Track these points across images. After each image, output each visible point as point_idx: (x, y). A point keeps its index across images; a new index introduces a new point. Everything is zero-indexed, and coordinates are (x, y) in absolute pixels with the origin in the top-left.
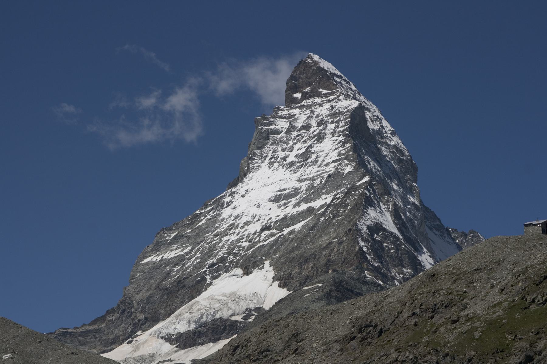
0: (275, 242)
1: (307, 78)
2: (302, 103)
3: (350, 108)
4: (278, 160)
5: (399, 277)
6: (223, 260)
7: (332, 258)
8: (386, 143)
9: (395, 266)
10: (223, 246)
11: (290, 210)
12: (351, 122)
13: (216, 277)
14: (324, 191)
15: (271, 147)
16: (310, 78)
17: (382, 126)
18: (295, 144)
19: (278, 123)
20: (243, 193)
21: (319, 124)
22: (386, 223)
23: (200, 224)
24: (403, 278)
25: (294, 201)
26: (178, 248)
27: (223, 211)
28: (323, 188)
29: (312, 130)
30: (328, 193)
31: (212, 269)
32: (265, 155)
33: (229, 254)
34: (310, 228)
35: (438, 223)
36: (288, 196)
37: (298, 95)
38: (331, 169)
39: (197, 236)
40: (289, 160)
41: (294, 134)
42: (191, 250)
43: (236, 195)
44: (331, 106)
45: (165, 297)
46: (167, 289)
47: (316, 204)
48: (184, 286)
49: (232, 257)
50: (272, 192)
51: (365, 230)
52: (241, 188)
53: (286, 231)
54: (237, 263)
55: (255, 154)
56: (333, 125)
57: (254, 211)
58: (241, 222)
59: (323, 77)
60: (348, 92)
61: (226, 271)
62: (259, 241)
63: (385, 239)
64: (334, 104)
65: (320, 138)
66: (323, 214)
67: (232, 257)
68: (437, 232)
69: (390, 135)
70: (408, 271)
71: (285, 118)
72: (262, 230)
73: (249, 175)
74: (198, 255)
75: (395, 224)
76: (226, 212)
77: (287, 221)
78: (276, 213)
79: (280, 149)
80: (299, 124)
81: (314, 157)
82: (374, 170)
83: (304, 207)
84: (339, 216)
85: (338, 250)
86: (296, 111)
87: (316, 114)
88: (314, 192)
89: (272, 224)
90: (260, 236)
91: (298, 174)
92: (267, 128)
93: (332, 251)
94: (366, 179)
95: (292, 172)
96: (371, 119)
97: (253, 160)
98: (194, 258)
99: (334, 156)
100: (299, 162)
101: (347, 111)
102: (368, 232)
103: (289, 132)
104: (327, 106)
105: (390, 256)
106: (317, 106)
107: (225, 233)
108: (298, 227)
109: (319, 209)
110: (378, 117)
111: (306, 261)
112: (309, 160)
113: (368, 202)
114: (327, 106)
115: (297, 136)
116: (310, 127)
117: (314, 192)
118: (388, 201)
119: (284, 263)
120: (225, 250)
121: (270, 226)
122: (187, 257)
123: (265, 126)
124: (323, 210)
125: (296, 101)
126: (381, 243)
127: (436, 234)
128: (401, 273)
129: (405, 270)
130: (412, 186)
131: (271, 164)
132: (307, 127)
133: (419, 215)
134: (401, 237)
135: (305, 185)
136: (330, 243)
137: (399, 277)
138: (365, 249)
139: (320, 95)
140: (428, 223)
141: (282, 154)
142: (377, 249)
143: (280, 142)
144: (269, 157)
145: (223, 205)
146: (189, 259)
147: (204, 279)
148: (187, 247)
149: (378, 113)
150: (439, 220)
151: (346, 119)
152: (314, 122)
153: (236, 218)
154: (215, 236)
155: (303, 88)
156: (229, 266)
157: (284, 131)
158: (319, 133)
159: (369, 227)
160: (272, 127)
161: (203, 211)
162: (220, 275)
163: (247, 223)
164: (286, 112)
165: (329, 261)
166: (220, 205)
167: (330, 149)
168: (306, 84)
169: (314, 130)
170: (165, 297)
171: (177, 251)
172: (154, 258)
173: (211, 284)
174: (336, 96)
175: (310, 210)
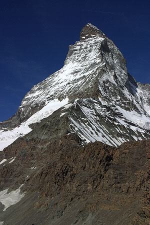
6: (51, 96)
9: (113, 96)
11: (78, 77)
21: (90, 47)
36: (76, 72)
38: (93, 62)
40: (79, 59)
47: (86, 74)
50: (72, 70)
52: (61, 70)
53: (75, 84)
55: (68, 58)
57: (66, 78)
65: (90, 51)
76: (56, 79)
77: (75, 81)
78: (72, 78)
83: (82, 75)
86: (83, 43)
94: (104, 64)
99: (95, 57)
103: (80, 50)
104: (94, 40)
114: (94, 40)
118: (112, 72)
132: (86, 48)
134: (117, 85)
138: (101, 90)
139: (91, 37)
141: (77, 58)
147: (44, 103)
149: (112, 43)
152: (89, 46)
159: (104, 82)
166: (53, 76)
167: (94, 56)
172: (30, 96)
175: (84, 77)
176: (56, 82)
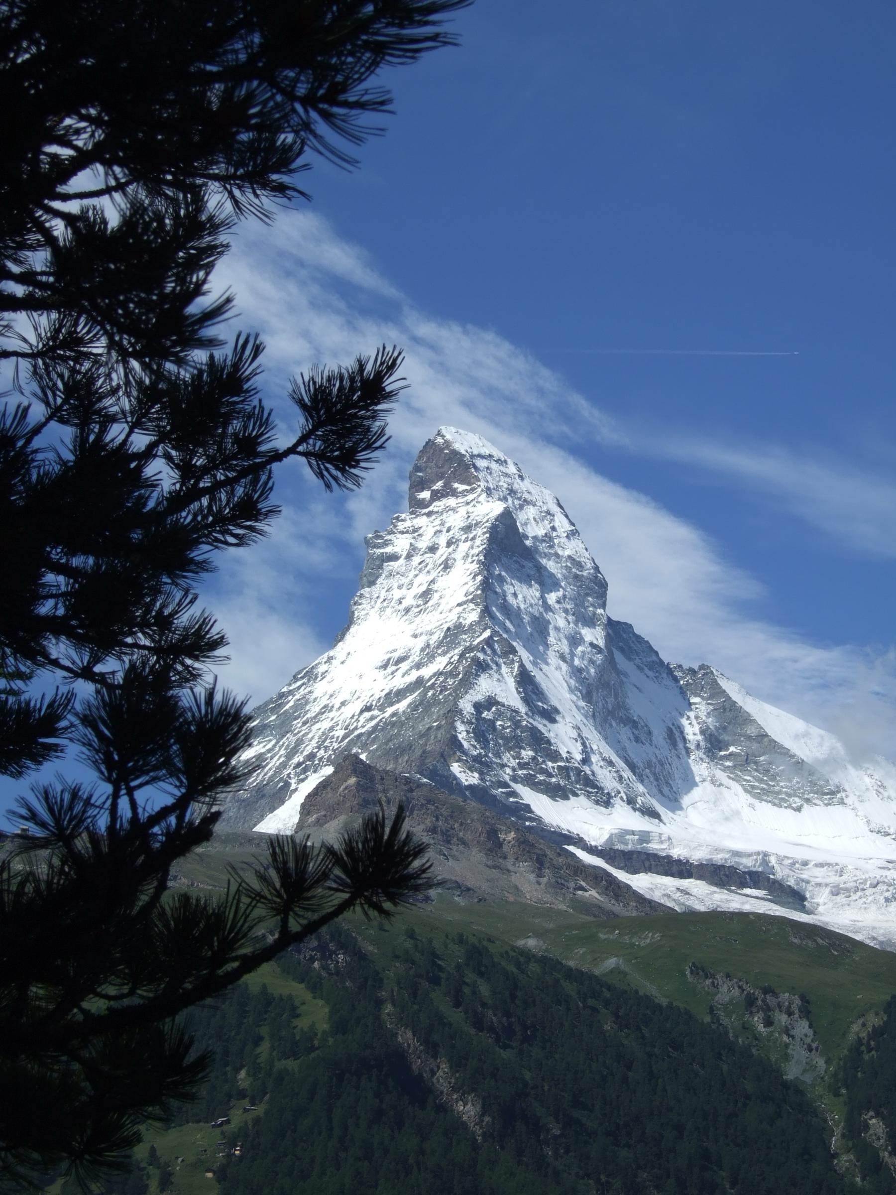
0: (375, 728)
1: (437, 466)
2: (431, 508)
3: (491, 515)
4: (392, 604)
5: (514, 763)
6: (311, 756)
7: (428, 748)
8: (557, 555)
9: (509, 749)
10: (312, 738)
11: (399, 682)
12: (490, 540)
13: (303, 780)
14: (439, 651)
15: (385, 582)
16: (442, 467)
17: (553, 529)
18: (416, 576)
19: (396, 542)
20: (343, 658)
21: (449, 544)
22: (503, 694)
23: (287, 707)
24: (519, 764)
25: (404, 666)
26: (259, 743)
27: (316, 685)
28: (438, 647)
29: (439, 552)
30: (444, 654)
31: (298, 770)
32: (376, 596)
33: (319, 748)
34: (414, 707)
35: (654, 658)
37: (425, 495)
38: (451, 619)
39: (283, 724)
40: (406, 603)
41: (416, 560)
42: (274, 746)
43: (333, 661)
44: (468, 513)
45: (242, 811)
46: (244, 801)
47: (427, 672)
48: (264, 796)
49: (322, 752)
51: (468, 709)
53: (390, 711)
54: (329, 759)
55: (362, 596)
56: (469, 543)
58: (337, 702)
59: (459, 464)
60: (499, 481)
61: (315, 772)
62: (356, 728)
63: (500, 716)
64: (471, 510)
65: (447, 566)
66: (432, 686)
67: (322, 752)
68: (650, 673)
69: (564, 540)
70: (527, 754)
71: (407, 532)
72: (362, 712)
73: (353, 629)
74: (282, 752)
75: (519, 693)
79: (395, 585)
80: (423, 544)
81: (436, 596)
82: (522, 606)
83: (414, 676)
84: (446, 689)
85: (435, 737)
86: (422, 521)
87: (447, 525)
88: (429, 654)
89: (374, 703)
90: (358, 720)
91: (413, 626)
92: (382, 551)
93: (428, 740)
94: (487, 634)
95: (408, 622)
96: (535, 519)
97: (360, 604)
98: (277, 757)
100: (418, 606)
101: (487, 521)
102: (473, 711)
104: (463, 511)
105: (503, 737)
106: (450, 512)
107: (316, 719)
108: (402, 706)
109: (430, 679)
110: (548, 512)
111: (403, 751)
112: (430, 604)
113: (482, 667)
114: (463, 511)
115: (420, 563)
116: (437, 548)
117: (429, 654)
118: (513, 662)
119: (380, 757)
120: (314, 743)
121: (371, 705)
122: (269, 755)
123: (379, 548)
124: (433, 680)
125: (423, 504)
126: (492, 723)
127: (648, 677)
128: (518, 756)
129: (523, 753)
130: (594, 614)
131: (383, 609)
132: (433, 549)
133: (599, 658)
135: (420, 643)
136: (430, 728)
137: (514, 763)
139: (454, 493)
140: (638, 661)
141: (397, 594)
142: (482, 731)
143: (398, 573)
144: (381, 600)
145: (316, 678)
146: (272, 758)
147: (287, 784)
148: (270, 741)
150: (656, 653)
151: (484, 533)
152: (442, 540)
153: (331, 696)
154: (304, 723)
155: (434, 482)
156: (319, 764)
157: (405, 554)
158: (447, 560)
160: (388, 550)
161: (291, 688)
162: (307, 777)
163: (343, 704)
164: (408, 524)
165: (424, 752)
168: (438, 476)
169: (443, 552)
170: (242, 811)
171: (258, 747)
173: (296, 790)
174: (475, 495)
175: (420, 682)
176: (324, 701)
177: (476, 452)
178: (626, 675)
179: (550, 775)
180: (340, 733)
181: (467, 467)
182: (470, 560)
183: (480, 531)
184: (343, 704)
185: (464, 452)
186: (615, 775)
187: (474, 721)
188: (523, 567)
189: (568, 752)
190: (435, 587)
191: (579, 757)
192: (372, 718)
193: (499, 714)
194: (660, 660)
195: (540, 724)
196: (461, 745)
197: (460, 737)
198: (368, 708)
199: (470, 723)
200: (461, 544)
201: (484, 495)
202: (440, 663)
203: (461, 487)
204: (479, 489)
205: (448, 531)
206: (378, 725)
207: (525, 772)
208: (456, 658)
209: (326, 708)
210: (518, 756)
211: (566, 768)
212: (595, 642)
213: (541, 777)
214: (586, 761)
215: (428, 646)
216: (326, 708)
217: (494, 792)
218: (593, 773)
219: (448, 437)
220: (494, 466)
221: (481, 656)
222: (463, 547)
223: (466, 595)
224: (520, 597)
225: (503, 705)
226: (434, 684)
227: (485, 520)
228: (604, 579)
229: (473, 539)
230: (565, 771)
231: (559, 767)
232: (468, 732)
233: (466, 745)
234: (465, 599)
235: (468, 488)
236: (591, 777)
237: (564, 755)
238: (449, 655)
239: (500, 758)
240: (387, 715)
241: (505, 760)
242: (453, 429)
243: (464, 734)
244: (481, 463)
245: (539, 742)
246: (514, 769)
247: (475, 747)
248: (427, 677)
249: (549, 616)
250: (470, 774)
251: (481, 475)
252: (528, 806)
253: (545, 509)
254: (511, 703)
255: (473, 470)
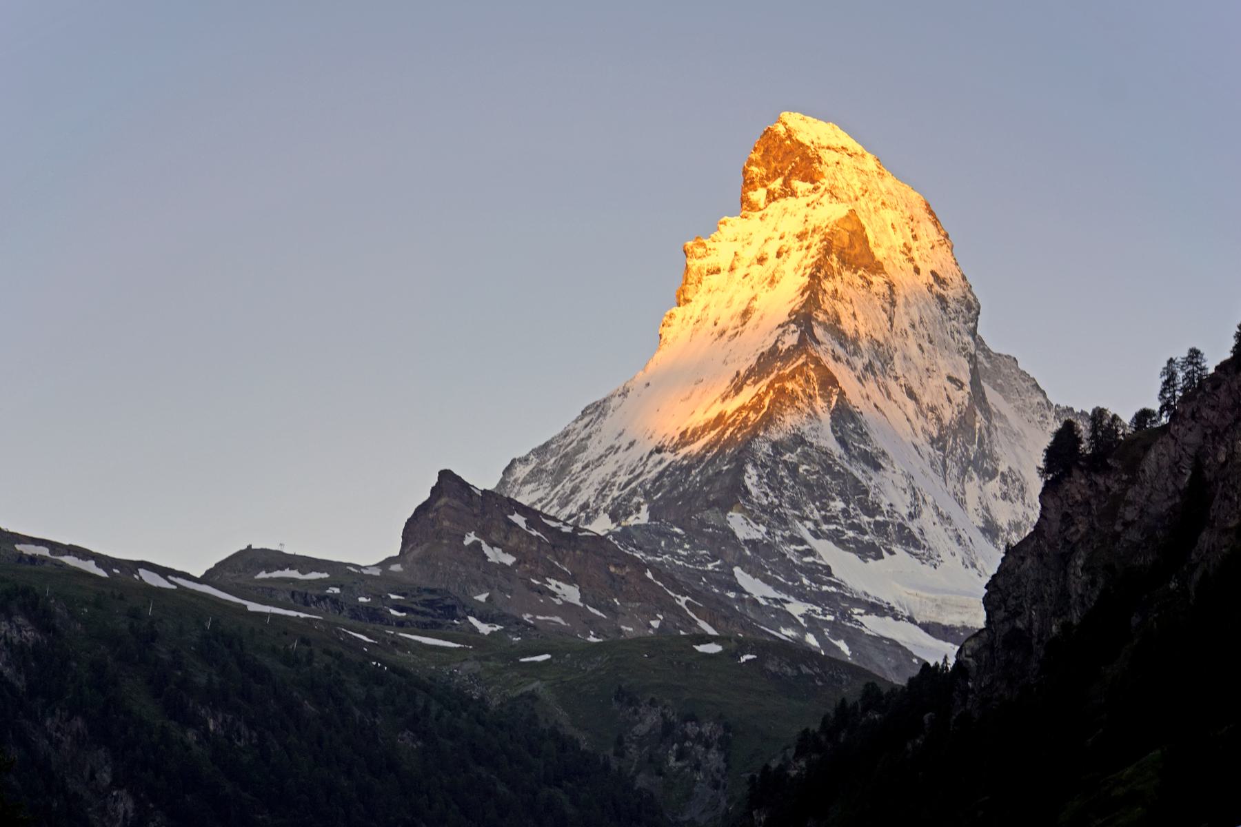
0: (661, 474)
2: (765, 212)
16: (782, 161)
21: (779, 255)
29: (767, 264)
47: (732, 406)
53: (683, 452)
59: (802, 159)
72: (651, 453)
74: (555, 501)
75: (834, 431)
84: (746, 427)
90: (645, 464)
104: (801, 217)
132: (761, 260)
137: (817, 515)
139: (794, 194)
152: (771, 251)
163: (632, 444)
169: (772, 261)
175: (720, 418)
177: (825, 144)
178: (1002, 417)
179: (864, 533)
180: (623, 478)
181: (811, 161)
182: (801, 272)
183: (817, 238)
184: (632, 444)
185: (808, 144)
186: (951, 534)
187: (769, 464)
188: (870, 283)
189: (891, 505)
190: (756, 304)
191: (904, 512)
192: (660, 462)
193: (806, 457)
194: (1048, 402)
195: (857, 470)
196: (748, 492)
197: (748, 482)
198: (659, 450)
199: (764, 466)
200: (793, 253)
201: (827, 196)
202: (747, 394)
203: (799, 185)
204: (823, 188)
205: (781, 238)
206: (666, 469)
207: (833, 527)
208: (764, 389)
209: (613, 449)
210: (824, 507)
211: (886, 524)
212: (955, 375)
213: (851, 534)
214: (912, 516)
215: (738, 374)
216: (613, 449)
217: (785, 548)
218: (922, 531)
219: (790, 125)
220: (846, 160)
221: (790, 386)
222: (796, 257)
223: (790, 315)
224: (860, 318)
225: (811, 445)
226: (735, 421)
227: (823, 226)
228: (975, 300)
229: (808, 248)
230: (880, 528)
231: (877, 523)
232: (760, 477)
233: (754, 491)
234: (787, 319)
235: (810, 186)
236: (918, 536)
237: (885, 508)
238: (758, 386)
239: (800, 509)
240: (679, 457)
241: (808, 511)
242: (798, 115)
243: (755, 479)
244: (829, 157)
245: (856, 492)
246: (816, 523)
247: (767, 495)
248: (729, 412)
249: (896, 342)
250: (755, 526)
251: (828, 171)
252: (828, 568)
253: (908, 214)
254: (823, 443)
255: (817, 165)
